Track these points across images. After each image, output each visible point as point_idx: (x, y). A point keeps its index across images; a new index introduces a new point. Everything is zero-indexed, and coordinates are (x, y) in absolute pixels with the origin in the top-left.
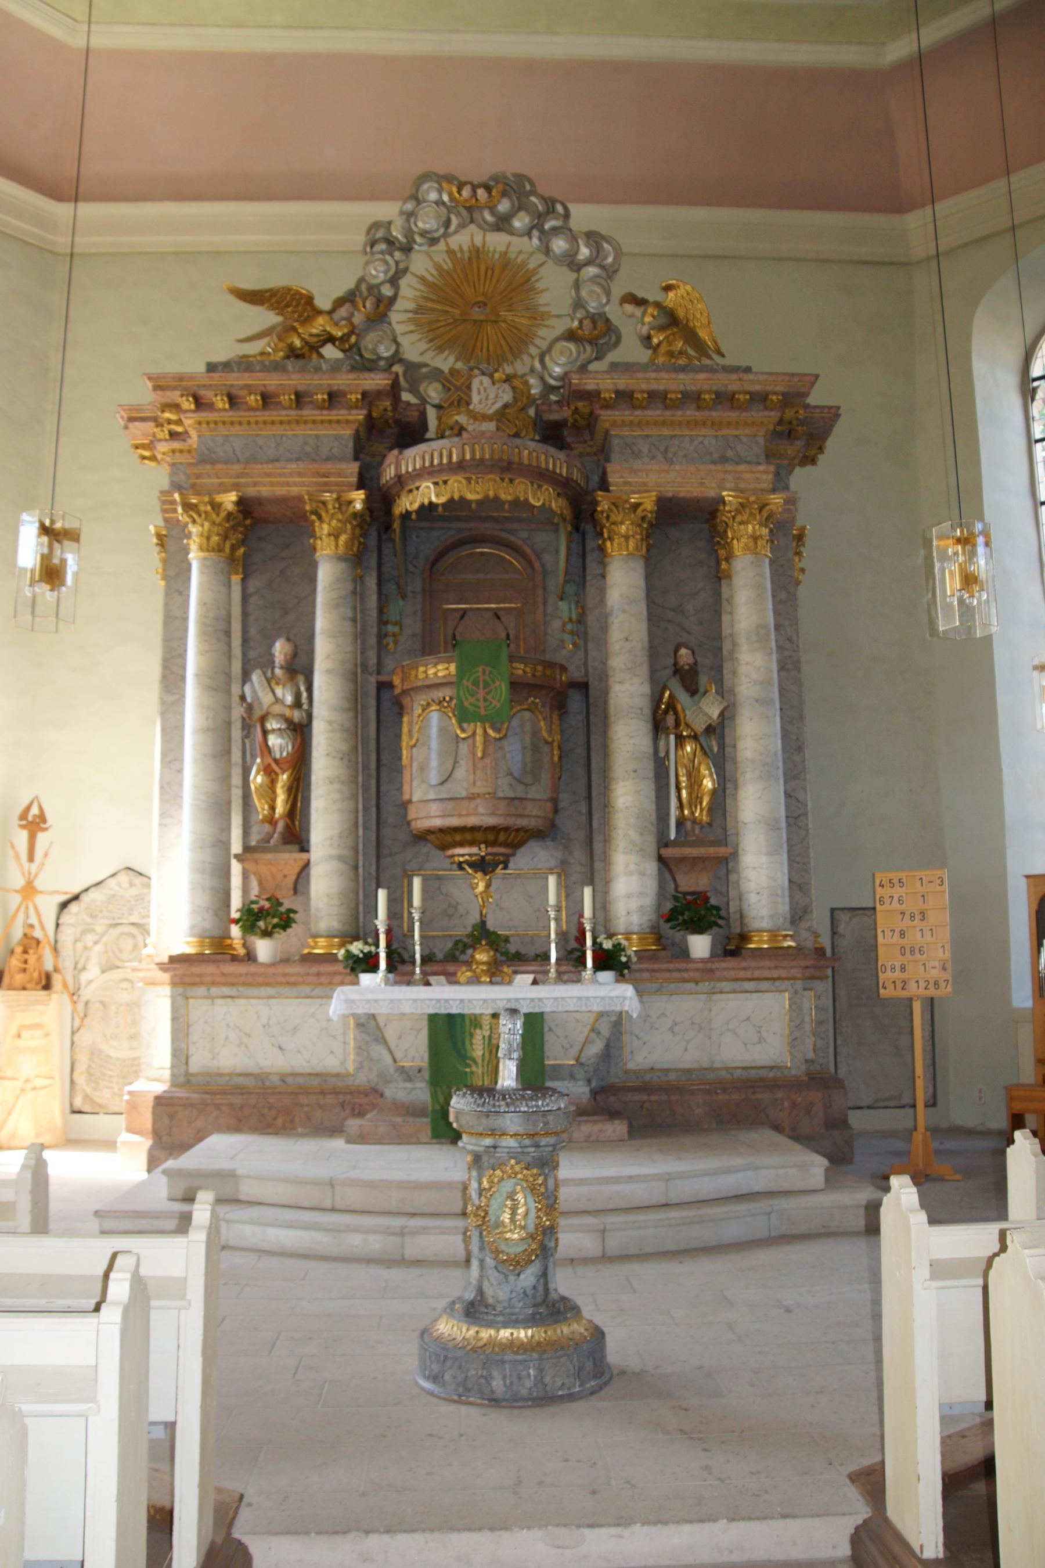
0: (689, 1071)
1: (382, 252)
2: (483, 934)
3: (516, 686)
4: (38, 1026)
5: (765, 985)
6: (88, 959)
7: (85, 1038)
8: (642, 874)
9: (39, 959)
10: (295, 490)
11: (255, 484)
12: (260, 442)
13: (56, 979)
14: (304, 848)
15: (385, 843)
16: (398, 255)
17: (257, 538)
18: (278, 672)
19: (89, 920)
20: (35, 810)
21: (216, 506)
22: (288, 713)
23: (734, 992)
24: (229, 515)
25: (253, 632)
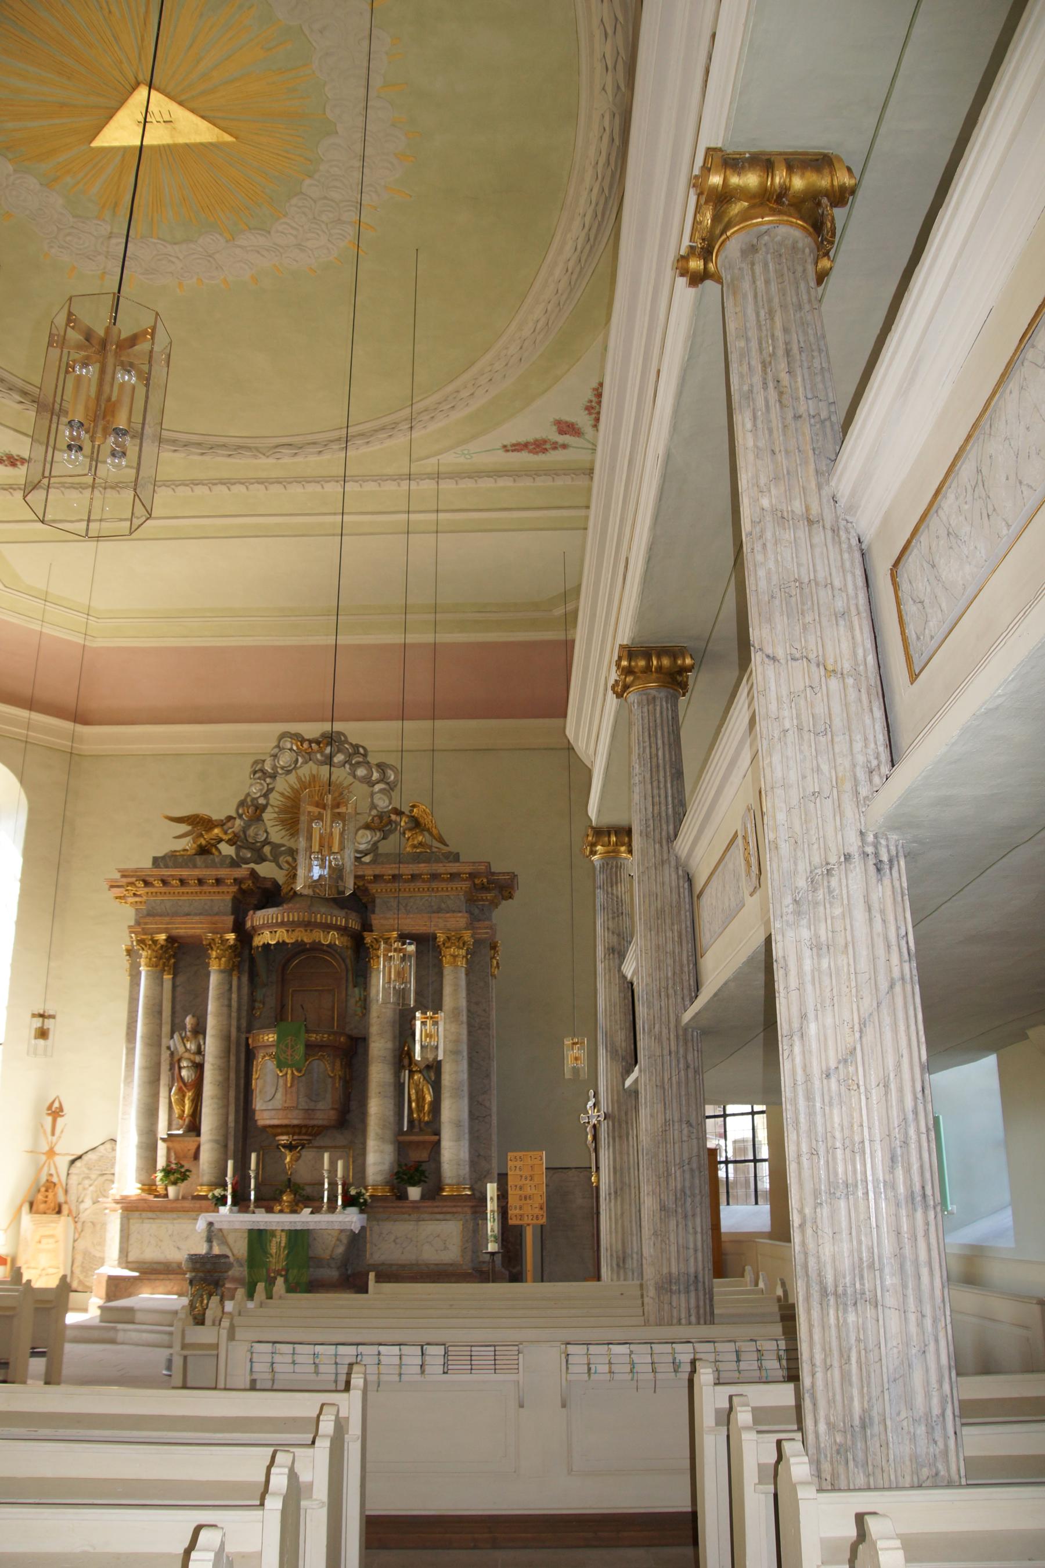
0: (403, 1266)
1: (259, 778)
2: (291, 1185)
3: (310, 1047)
4: (52, 1236)
5: (448, 1216)
6: (85, 1195)
7: (81, 1245)
8: (382, 1152)
9: (55, 1195)
10: (198, 931)
11: (177, 928)
12: (180, 903)
13: (65, 1209)
14: (199, 1135)
15: (244, 1133)
16: (268, 780)
17: (177, 957)
18: (188, 1034)
19: (87, 1171)
20: (56, 1105)
21: (155, 942)
22: (192, 1057)
23: (431, 1220)
24: (162, 946)
25: (178, 1007)
